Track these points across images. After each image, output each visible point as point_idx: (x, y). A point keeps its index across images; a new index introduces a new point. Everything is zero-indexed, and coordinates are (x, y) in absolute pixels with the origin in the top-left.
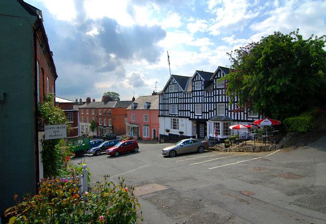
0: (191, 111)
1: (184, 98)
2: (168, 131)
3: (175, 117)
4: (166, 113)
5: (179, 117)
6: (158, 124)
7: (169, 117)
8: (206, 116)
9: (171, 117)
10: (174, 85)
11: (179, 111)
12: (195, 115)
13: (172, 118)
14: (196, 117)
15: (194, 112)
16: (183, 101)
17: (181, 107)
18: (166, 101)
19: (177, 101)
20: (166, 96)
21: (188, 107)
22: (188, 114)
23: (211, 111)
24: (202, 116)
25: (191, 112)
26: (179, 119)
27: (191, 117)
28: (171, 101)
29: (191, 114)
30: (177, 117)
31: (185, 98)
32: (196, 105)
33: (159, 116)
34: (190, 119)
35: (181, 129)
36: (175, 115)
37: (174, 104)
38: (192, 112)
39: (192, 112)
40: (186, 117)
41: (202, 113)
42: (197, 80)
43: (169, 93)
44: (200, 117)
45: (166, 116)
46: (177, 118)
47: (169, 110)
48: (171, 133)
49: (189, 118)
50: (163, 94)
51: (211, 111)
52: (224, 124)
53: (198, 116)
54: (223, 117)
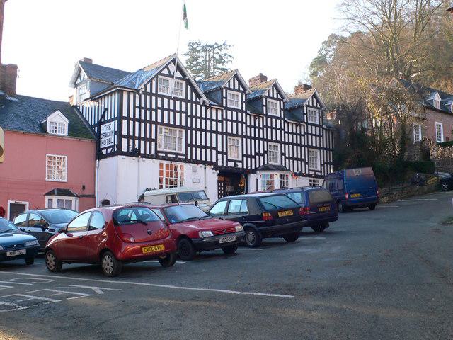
0: (220, 149)
4: (145, 147)
7: (158, 158)
8: (250, 164)
9: (163, 158)
11: (187, 145)
12: (227, 160)
13: (165, 162)
14: (231, 164)
15: (226, 153)
17: (198, 138)
21: (210, 140)
22: (210, 156)
23: (259, 154)
24: (242, 162)
25: (218, 153)
27: (220, 164)
29: (220, 156)
30: (180, 160)
36: (177, 154)
37: (174, 126)
38: (222, 153)
39: (222, 153)
40: (205, 163)
41: (243, 156)
44: (240, 165)
45: (145, 156)
46: (178, 164)
49: (216, 167)
51: (259, 154)
53: (235, 161)
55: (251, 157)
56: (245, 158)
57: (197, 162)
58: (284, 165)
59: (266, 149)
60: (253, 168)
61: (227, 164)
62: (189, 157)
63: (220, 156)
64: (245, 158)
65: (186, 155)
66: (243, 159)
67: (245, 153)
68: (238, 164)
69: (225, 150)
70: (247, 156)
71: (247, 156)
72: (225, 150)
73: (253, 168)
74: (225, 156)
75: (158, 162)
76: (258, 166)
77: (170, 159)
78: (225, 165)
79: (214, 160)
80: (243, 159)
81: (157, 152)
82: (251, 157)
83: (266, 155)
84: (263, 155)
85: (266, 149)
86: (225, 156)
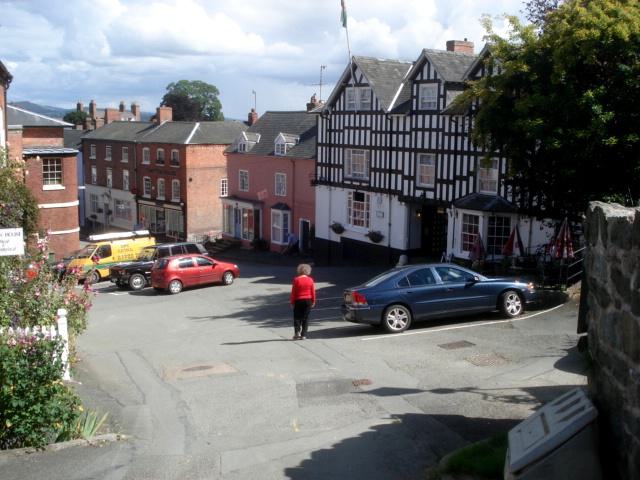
1: (335, 131)
2: (338, 229)
4: (336, 175)
6: (312, 204)
8: (446, 193)
9: (349, 186)
10: (357, 89)
11: (371, 169)
12: (416, 188)
14: (419, 193)
15: (414, 178)
16: (382, 140)
17: (380, 159)
18: (336, 138)
19: (366, 138)
20: (338, 122)
21: (401, 161)
22: (397, 182)
23: (461, 178)
24: (434, 190)
25: (404, 178)
27: (406, 193)
28: (349, 137)
29: (406, 182)
30: (364, 188)
31: (391, 132)
32: (419, 155)
33: (315, 183)
34: (402, 198)
35: (378, 225)
36: (361, 181)
37: (359, 147)
38: (409, 178)
39: (409, 178)
40: (390, 192)
42: (425, 77)
43: (344, 113)
44: (430, 195)
47: (342, 167)
49: (399, 194)
50: (327, 113)
51: (461, 178)
52: (491, 220)
53: (425, 189)
54: (492, 197)
55: (448, 182)
56: (439, 185)
58: (502, 195)
59: (472, 169)
62: (372, 185)
63: (406, 182)
64: (439, 185)
65: (369, 182)
66: (436, 186)
67: (439, 177)
70: (441, 181)
71: (441, 181)
73: (450, 199)
74: (412, 182)
75: (347, 190)
78: (412, 195)
79: (399, 188)
80: (436, 186)
81: (344, 179)
82: (448, 182)
83: (471, 179)
84: (467, 178)
85: (472, 169)
86: (412, 182)
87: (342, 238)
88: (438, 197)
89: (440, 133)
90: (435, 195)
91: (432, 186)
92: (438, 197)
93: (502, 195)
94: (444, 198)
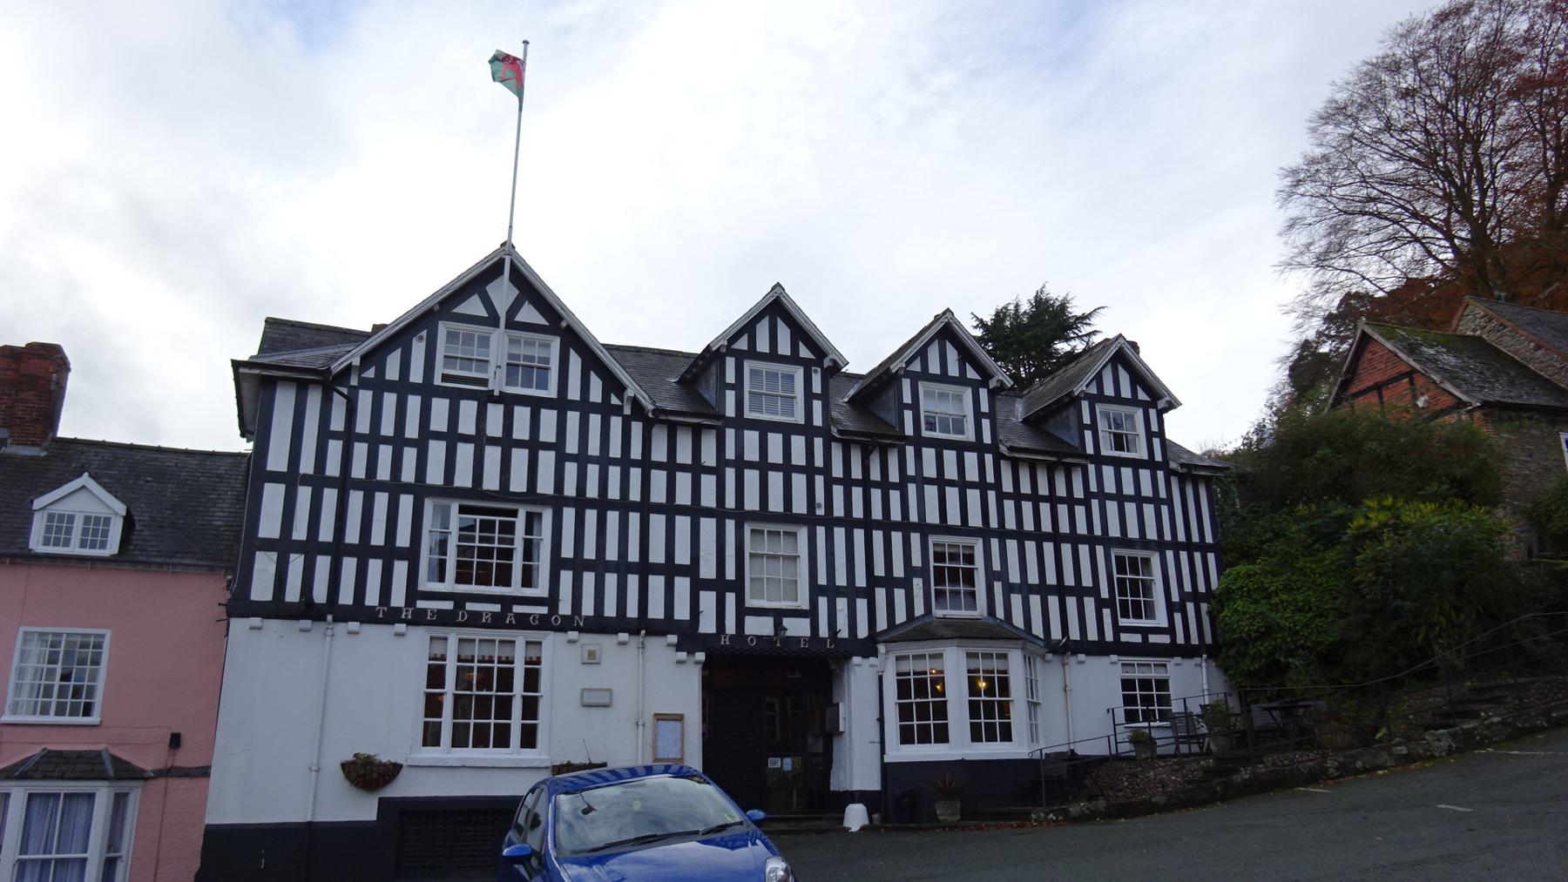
0: (708, 571)
3: (497, 622)
5: (544, 624)
7: (419, 619)
8: (847, 618)
9: (444, 619)
12: (742, 612)
14: (758, 627)
15: (738, 586)
23: (889, 582)
24: (812, 614)
26: (552, 643)
27: (707, 625)
30: (523, 622)
38: (720, 585)
39: (720, 585)
40: (644, 627)
44: (798, 628)
46: (521, 638)
48: (404, 788)
51: (889, 582)
53: (778, 615)
56: (823, 602)
57: (599, 625)
58: (1000, 614)
60: (863, 632)
61: (740, 624)
62: (565, 608)
67: (822, 580)
68: (787, 622)
69: (730, 574)
70: (832, 591)
72: (730, 574)
73: (863, 632)
74: (730, 598)
76: (882, 625)
77: (475, 620)
78: (731, 628)
79: (682, 612)
86: (730, 598)
87: (384, 804)
88: (824, 631)
89: (819, 480)
90: (815, 627)
91: (803, 603)
92: (824, 631)
93: (1000, 614)
94: (844, 634)
